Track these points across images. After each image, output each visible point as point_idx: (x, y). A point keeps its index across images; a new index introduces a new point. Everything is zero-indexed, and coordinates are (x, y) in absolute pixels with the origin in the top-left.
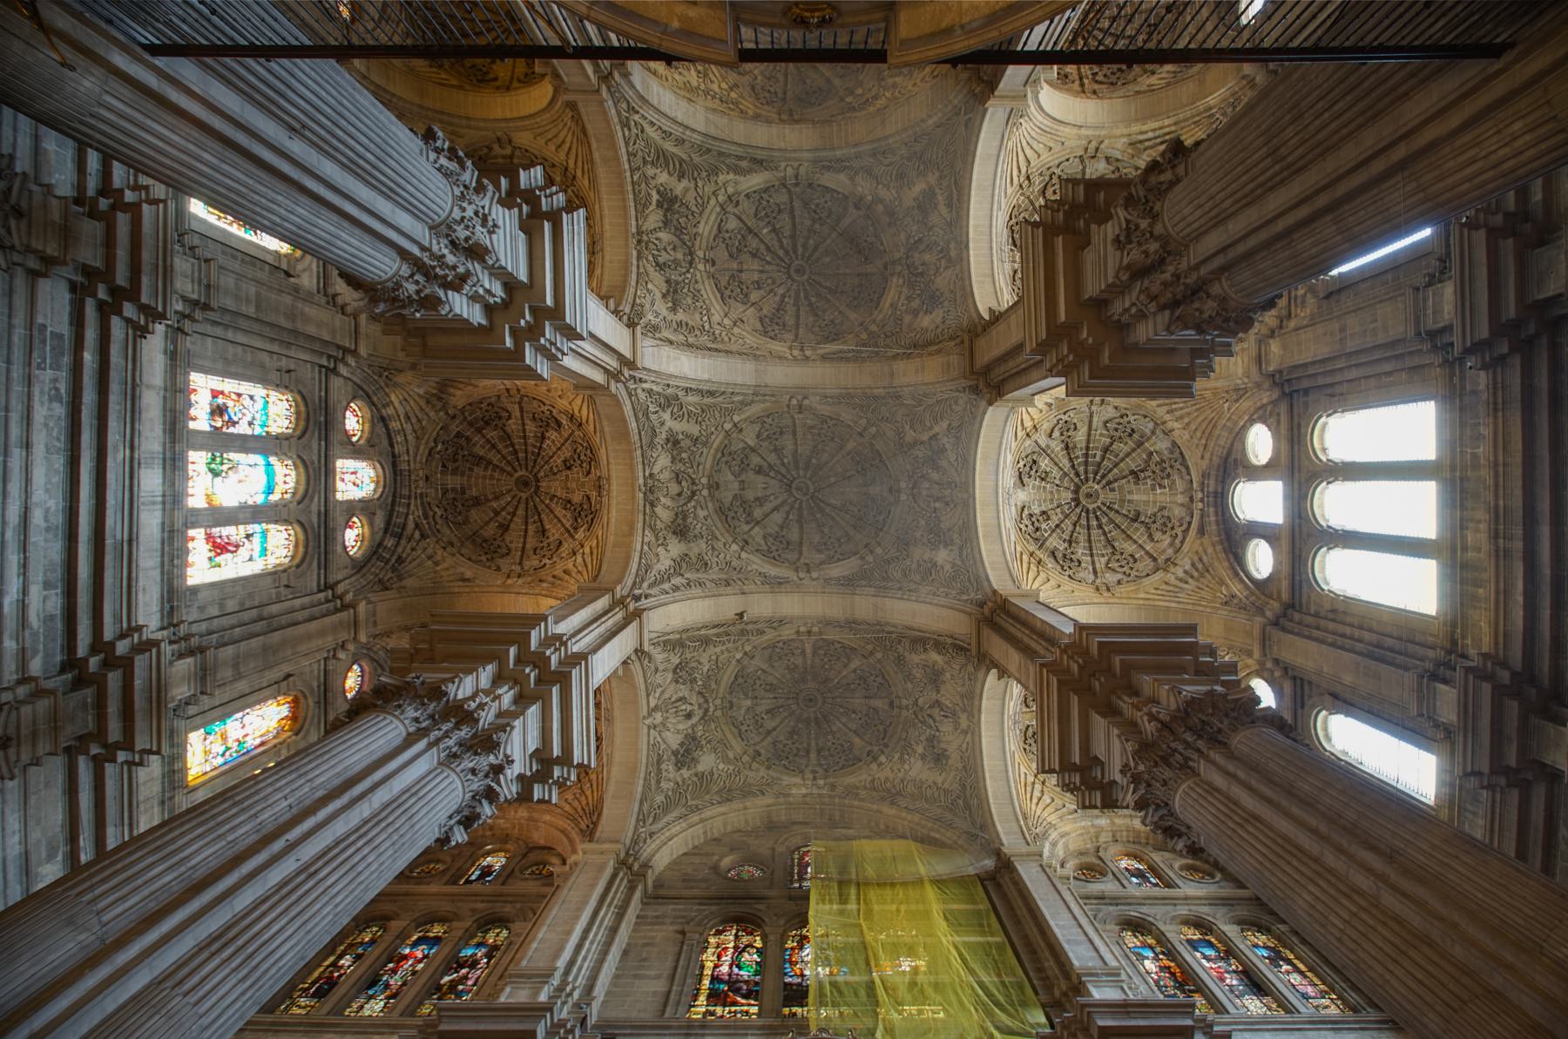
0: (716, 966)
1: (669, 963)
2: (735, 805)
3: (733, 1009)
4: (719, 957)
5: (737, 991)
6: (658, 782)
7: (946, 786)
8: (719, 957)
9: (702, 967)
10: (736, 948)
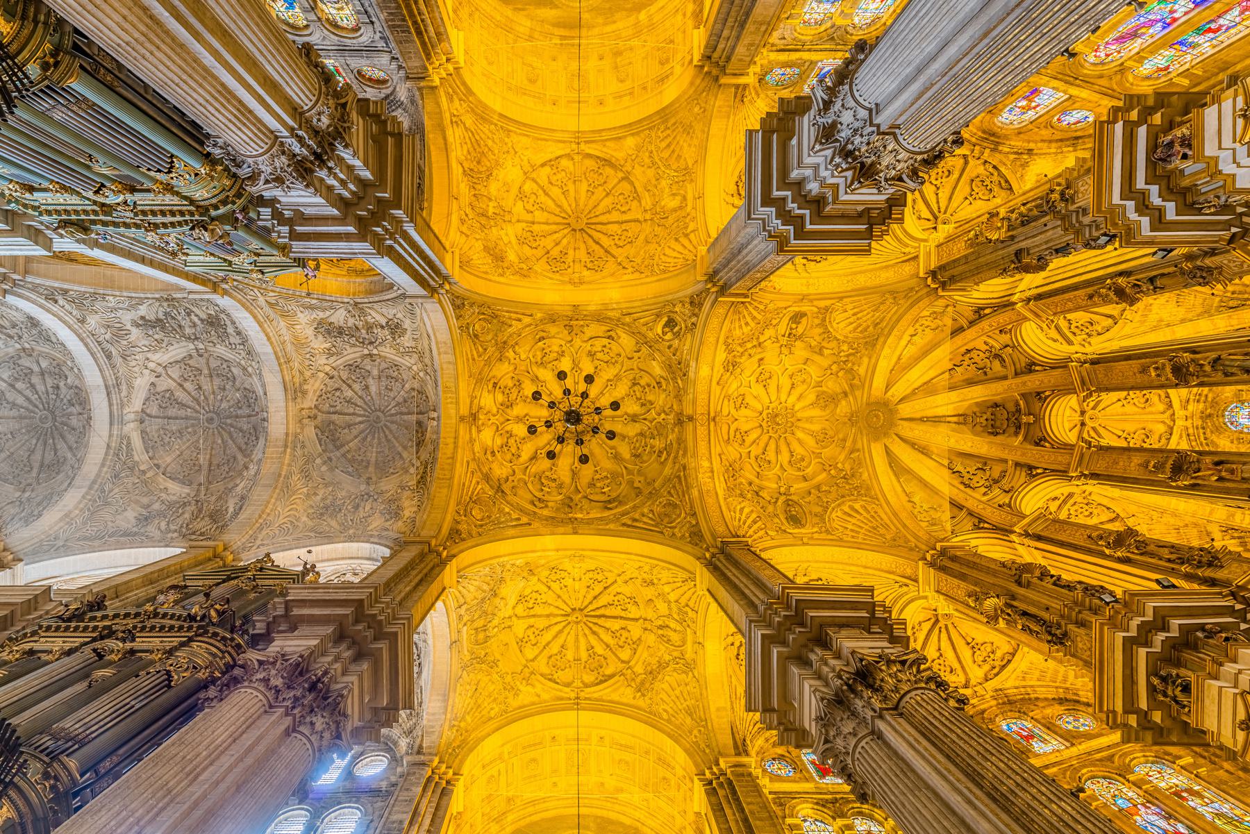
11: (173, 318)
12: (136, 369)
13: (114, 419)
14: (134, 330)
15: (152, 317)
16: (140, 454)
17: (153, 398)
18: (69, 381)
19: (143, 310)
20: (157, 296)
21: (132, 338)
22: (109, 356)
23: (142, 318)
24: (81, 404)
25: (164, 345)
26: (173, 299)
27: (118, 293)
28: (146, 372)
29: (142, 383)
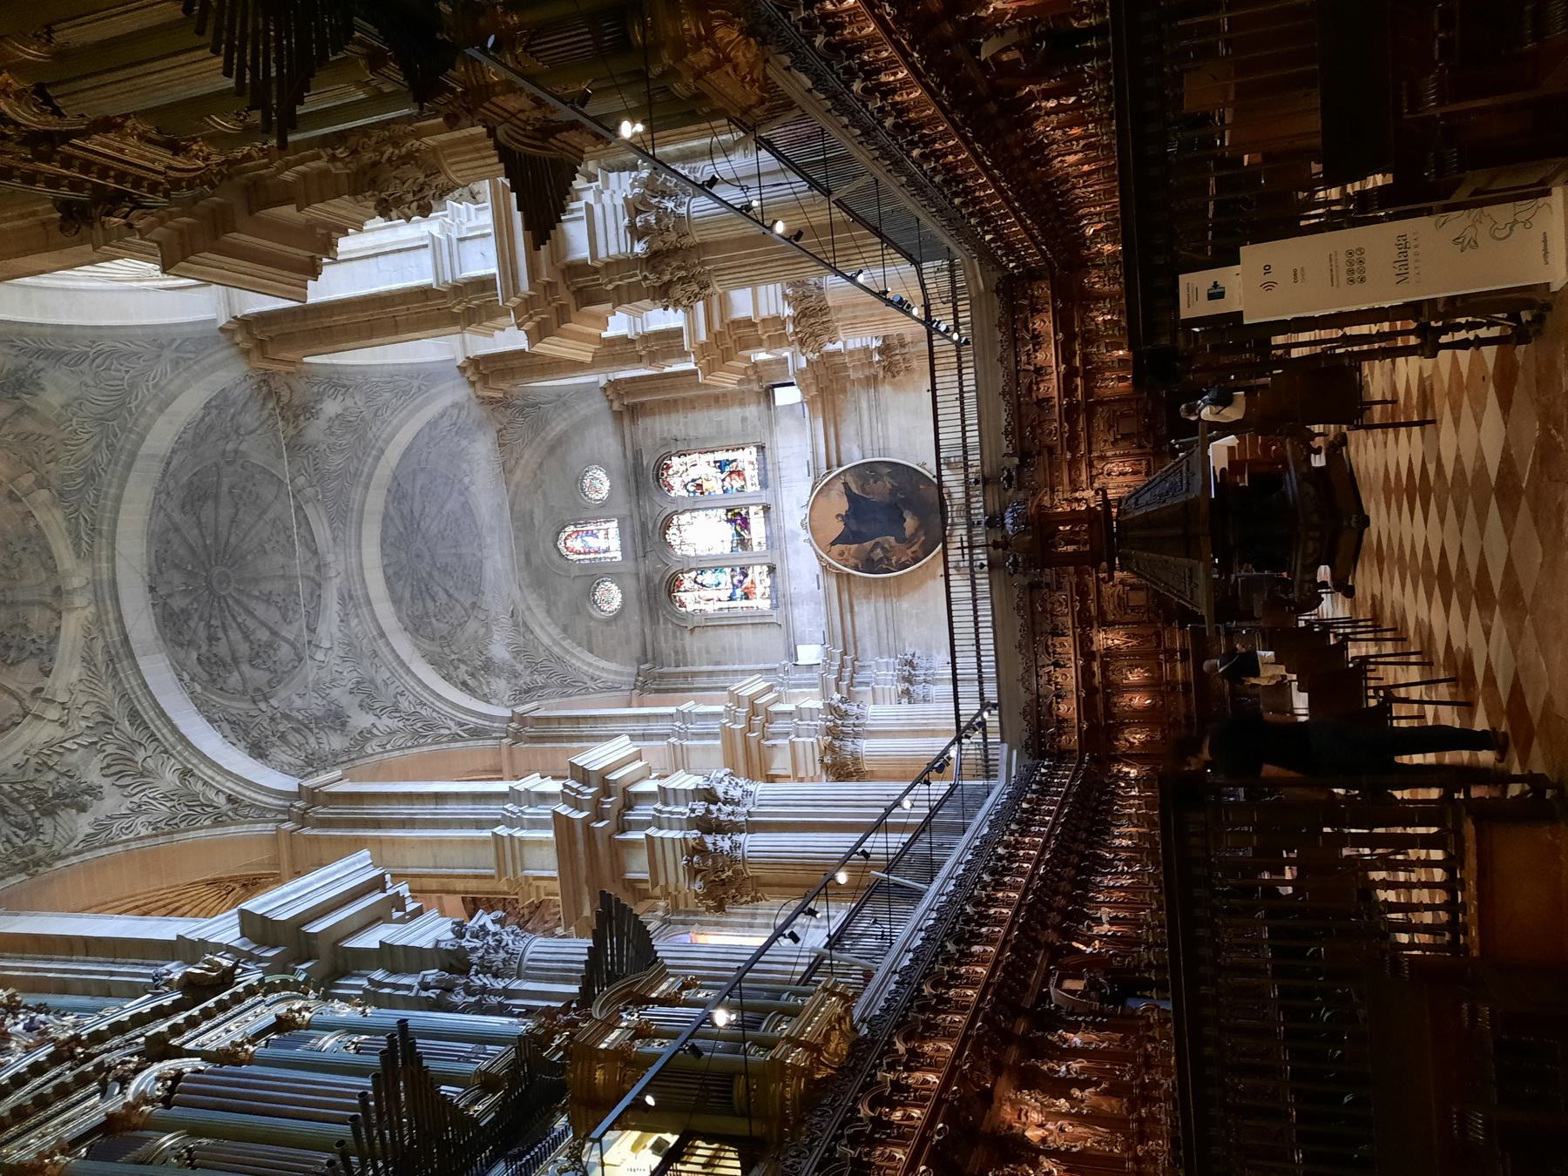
1: (726, 631)
2: (529, 620)
3: (757, 582)
5: (741, 582)
6: (542, 688)
7: (505, 421)
9: (721, 609)
11: (22, 827)
12: (82, 699)
13: (107, 593)
14: (94, 777)
15: (66, 815)
16: (52, 521)
17: (43, 644)
18: (195, 656)
19: (83, 824)
20: (59, 864)
21: (97, 762)
22: (134, 716)
23: (82, 809)
24: (171, 615)
25: (33, 761)
26: (24, 868)
27: (133, 845)
28: (62, 697)
29: (68, 674)
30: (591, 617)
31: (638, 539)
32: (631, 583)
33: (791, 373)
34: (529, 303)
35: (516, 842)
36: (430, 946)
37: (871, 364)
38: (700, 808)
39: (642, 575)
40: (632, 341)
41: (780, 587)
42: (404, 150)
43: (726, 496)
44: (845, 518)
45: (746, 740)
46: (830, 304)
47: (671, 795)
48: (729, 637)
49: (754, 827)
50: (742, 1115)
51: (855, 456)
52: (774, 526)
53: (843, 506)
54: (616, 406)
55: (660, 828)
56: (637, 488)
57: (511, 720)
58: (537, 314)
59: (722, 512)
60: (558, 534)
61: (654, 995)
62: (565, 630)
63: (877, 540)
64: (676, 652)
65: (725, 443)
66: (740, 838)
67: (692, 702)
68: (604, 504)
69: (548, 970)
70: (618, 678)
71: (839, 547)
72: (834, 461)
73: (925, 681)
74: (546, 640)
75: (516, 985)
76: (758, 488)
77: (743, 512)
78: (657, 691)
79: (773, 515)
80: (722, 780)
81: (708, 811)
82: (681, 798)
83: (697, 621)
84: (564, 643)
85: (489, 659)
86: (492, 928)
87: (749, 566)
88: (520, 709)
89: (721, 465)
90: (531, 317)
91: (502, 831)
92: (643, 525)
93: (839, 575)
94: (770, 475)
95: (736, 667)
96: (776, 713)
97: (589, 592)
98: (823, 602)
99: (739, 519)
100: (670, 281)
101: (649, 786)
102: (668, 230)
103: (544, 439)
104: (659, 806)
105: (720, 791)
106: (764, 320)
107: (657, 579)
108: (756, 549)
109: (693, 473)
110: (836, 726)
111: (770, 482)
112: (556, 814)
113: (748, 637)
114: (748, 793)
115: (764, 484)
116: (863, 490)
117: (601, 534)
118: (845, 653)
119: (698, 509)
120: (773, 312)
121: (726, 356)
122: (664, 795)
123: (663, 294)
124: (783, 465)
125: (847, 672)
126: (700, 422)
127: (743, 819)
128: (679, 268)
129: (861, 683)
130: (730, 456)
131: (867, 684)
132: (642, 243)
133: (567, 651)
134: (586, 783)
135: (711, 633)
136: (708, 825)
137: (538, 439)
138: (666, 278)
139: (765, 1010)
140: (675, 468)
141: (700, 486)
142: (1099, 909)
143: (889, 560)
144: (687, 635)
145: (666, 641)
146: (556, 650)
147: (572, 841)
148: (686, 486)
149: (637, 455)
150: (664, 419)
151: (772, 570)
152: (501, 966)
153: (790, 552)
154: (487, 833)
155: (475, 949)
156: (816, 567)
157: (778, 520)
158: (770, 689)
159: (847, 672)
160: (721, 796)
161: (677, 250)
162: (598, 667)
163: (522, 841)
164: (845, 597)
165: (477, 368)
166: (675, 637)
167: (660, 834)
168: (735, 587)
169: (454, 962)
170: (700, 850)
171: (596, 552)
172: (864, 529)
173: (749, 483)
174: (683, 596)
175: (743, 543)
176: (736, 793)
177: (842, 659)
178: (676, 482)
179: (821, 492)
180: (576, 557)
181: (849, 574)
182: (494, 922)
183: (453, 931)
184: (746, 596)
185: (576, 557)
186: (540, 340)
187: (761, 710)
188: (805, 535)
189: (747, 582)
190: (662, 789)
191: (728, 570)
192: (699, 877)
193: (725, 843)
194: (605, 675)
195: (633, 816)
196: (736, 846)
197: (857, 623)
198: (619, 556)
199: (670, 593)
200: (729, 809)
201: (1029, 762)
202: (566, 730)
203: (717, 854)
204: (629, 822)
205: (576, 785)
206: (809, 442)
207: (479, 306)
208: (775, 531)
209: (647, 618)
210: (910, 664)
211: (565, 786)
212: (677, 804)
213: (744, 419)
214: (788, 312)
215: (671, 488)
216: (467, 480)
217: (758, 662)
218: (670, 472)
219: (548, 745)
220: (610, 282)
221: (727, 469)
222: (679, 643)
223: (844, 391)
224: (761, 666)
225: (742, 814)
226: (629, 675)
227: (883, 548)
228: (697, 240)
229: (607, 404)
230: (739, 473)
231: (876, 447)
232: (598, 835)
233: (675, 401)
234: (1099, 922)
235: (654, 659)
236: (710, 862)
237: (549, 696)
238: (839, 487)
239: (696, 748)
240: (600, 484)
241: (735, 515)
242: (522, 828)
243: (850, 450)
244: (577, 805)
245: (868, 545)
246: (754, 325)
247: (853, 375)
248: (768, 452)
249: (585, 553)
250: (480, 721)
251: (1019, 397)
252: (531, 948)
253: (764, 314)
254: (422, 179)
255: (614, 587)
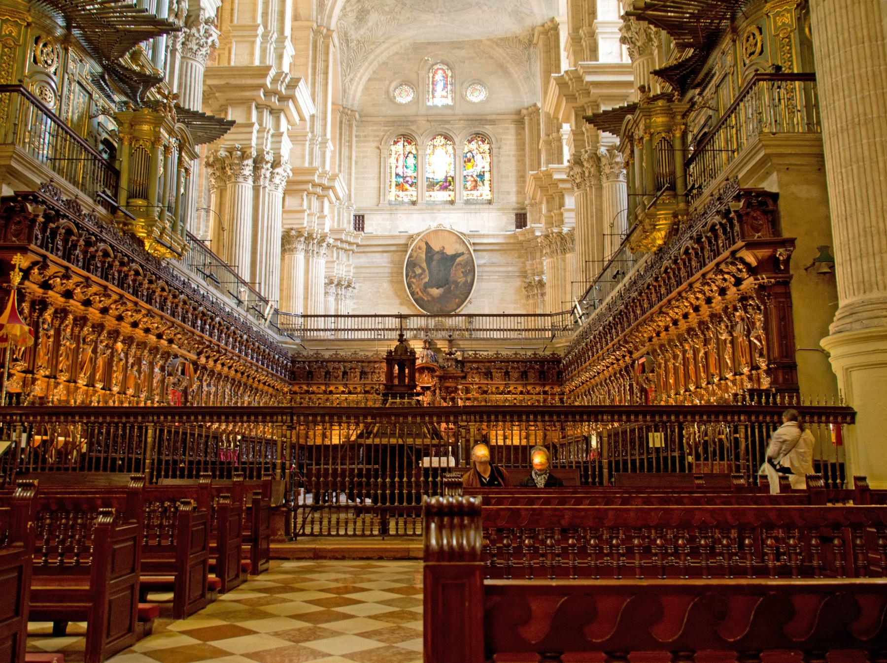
0: (397, 167)
1: (377, 170)
4: (397, 160)
5: (407, 182)
8: (397, 160)
10: (404, 154)
30: (391, 82)
31: (439, 118)
32: (411, 111)
33: (533, 225)
34: (580, 79)
35: (252, 39)
36: (202, 5)
37: (534, 274)
38: (269, 158)
39: (416, 118)
40: (558, 131)
41: (402, 208)
42: (653, 36)
43: (462, 178)
44: (442, 252)
45: (307, 182)
46: (568, 255)
47: (277, 139)
48: (373, 172)
49: (256, 189)
50: (128, 203)
51: (479, 260)
52: (441, 207)
53: (450, 251)
54: (524, 112)
55: (258, 132)
56: (472, 120)
57: (328, 30)
58: (573, 83)
59: (452, 174)
60: (447, 65)
61: (183, 154)
62: (385, 63)
63: (427, 271)
64: (365, 136)
65: (495, 180)
66: (250, 181)
67: (332, 149)
68: (463, 97)
69: (186, 75)
70: (351, 97)
71: (424, 246)
72: (477, 248)
73: (337, 294)
74: (378, 51)
75: (178, 56)
76: (465, 198)
77: (451, 187)
78: (341, 122)
79: (447, 206)
80: (285, 171)
81: (267, 162)
82: (276, 146)
83: (385, 152)
84: (376, 62)
85: (368, 12)
86: (210, 41)
87: (417, 188)
88: (335, 35)
89: (481, 176)
90: (571, 79)
91: (261, 30)
92: (448, 122)
93: (406, 245)
94: (473, 207)
95: (353, 175)
96: (323, 202)
97: (407, 82)
98: (391, 234)
99: (447, 184)
100: (583, 166)
101: (284, 126)
102: (611, 168)
103: (508, 62)
104: (272, 132)
105: (278, 170)
106: (562, 214)
107: (413, 128)
108: (427, 194)
109: (478, 157)
110: (313, 239)
111: (468, 207)
112: (269, 68)
113: (374, 184)
114: (277, 187)
115: (468, 202)
116: (458, 264)
117: (444, 94)
118: (358, 245)
119: (455, 158)
120: (566, 220)
121: (543, 189)
122: (278, 135)
123: (577, 161)
124: (478, 215)
125: (346, 246)
126: (509, 165)
127: (262, 183)
128: (590, 173)
129: (338, 254)
130: (487, 183)
131: (338, 258)
132: (605, 152)
133: (370, 65)
134: (288, 87)
135: (376, 160)
136: (258, 163)
137: (508, 58)
138: (585, 164)
139: (175, 215)
140: (482, 146)
141: (469, 161)
142: (214, 385)
143: (414, 277)
144: (376, 144)
145: (373, 130)
146: (372, 57)
147: (252, 76)
148: (470, 151)
149: (493, 122)
150: (513, 142)
151: (414, 203)
152: (189, 47)
153: (424, 215)
154: (259, 20)
155: (199, 31)
156: (412, 232)
157: (444, 209)
158: (338, 198)
159: (346, 246)
160: (276, 171)
161: (600, 172)
162: (358, 83)
163: (254, 42)
164: (393, 248)
165: (552, 29)
166: (375, 136)
167: (255, 132)
168: (404, 178)
169: (192, 19)
170: (244, 156)
171: (433, 89)
172: (434, 263)
173: (469, 192)
174: (401, 144)
175: (432, 185)
176: (277, 180)
177: (354, 244)
178: (473, 146)
179: (459, 238)
180: (431, 75)
181: (407, 251)
182: (213, 41)
183: (209, 18)
184: (397, 185)
185: (431, 75)
186: (557, 84)
187: (326, 193)
188: (433, 226)
189: (407, 186)
190: (281, 135)
191: (415, 175)
192: (228, 154)
193: (248, 171)
194: (353, 88)
195: (266, 113)
196: (245, 178)
197: (377, 254)
198: (430, 103)
199: (404, 136)
200: (268, 175)
201: (290, 355)
202: (320, 66)
203: (241, 167)
204: (262, 112)
205: (287, 81)
206: (491, 233)
207: (582, 46)
208: (438, 207)
209: (389, 119)
210: (349, 286)
211: (287, 74)
212: (272, 142)
213: (508, 193)
214: (565, 230)
215: (470, 142)
216: (485, 8)
217: (355, 189)
218: (480, 143)
219: (311, 52)
220: (587, 130)
221: (479, 179)
222: (371, 139)
223: (520, 257)
224: (353, 190)
225: (264, 183)
226: (352, 105)
227: (421, 274)
228: (604, 185)
229: (526, 105)
230: (475, 187)
231: (484, 274)
232: (255, 93)
233: (524, 150)
234: (209, 385)
235: (362, 121)
236: (237, 162)
237: (342, 50)
238: (461, 249)
239: (304, 150)
240: (476, 96)
241: (450, 182)
242: (262, 43)
243: (483, 258)
244: (275, 81)
245: (424, 265)
246: (560, 208)
247: (529, 263)
248: (487, 206)
249: (433, 81)
250: (328, 8)
251: (494, 362)
252: (198, 65)
253: (566, 215)
254: (639, 44)
255: (409, 99)
